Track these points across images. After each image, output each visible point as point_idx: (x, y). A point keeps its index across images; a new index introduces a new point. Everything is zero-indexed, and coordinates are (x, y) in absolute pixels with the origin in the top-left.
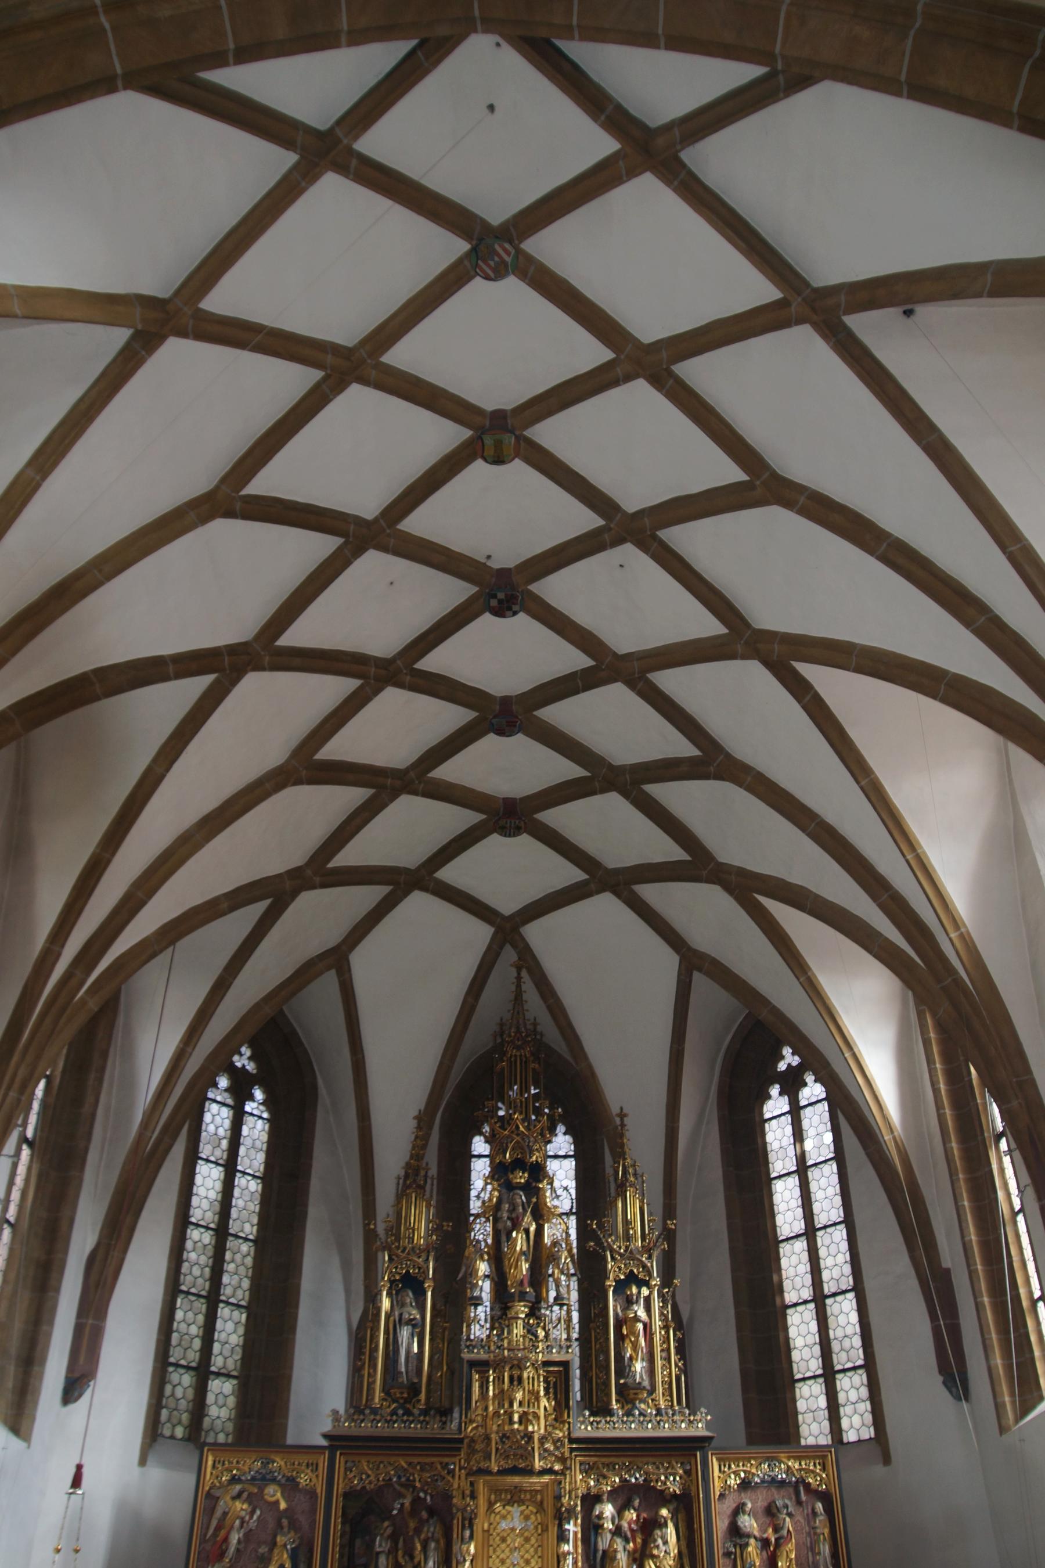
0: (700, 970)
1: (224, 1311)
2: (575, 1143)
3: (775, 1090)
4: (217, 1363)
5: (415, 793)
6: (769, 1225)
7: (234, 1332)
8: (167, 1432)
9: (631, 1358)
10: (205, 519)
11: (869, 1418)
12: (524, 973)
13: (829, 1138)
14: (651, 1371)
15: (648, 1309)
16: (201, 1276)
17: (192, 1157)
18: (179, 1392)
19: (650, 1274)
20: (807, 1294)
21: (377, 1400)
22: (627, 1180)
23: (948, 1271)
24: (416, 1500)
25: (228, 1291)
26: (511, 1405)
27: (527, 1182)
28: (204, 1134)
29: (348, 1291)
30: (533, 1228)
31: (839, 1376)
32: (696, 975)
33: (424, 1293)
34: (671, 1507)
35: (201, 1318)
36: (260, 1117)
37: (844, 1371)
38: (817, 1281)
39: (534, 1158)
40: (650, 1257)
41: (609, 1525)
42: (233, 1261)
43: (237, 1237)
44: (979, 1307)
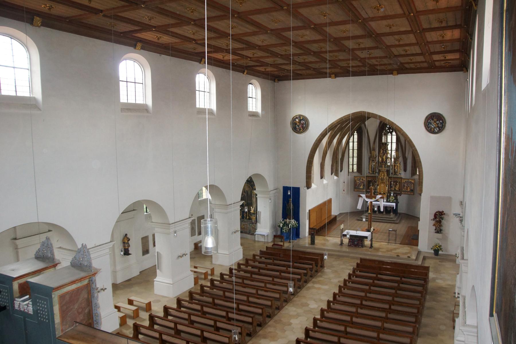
1: (354, 158)
4: (354, 164)
8: (350, 171)
24: (375, 181)
30: (386, 155)
35: (352, 160)
41: (392, 184)
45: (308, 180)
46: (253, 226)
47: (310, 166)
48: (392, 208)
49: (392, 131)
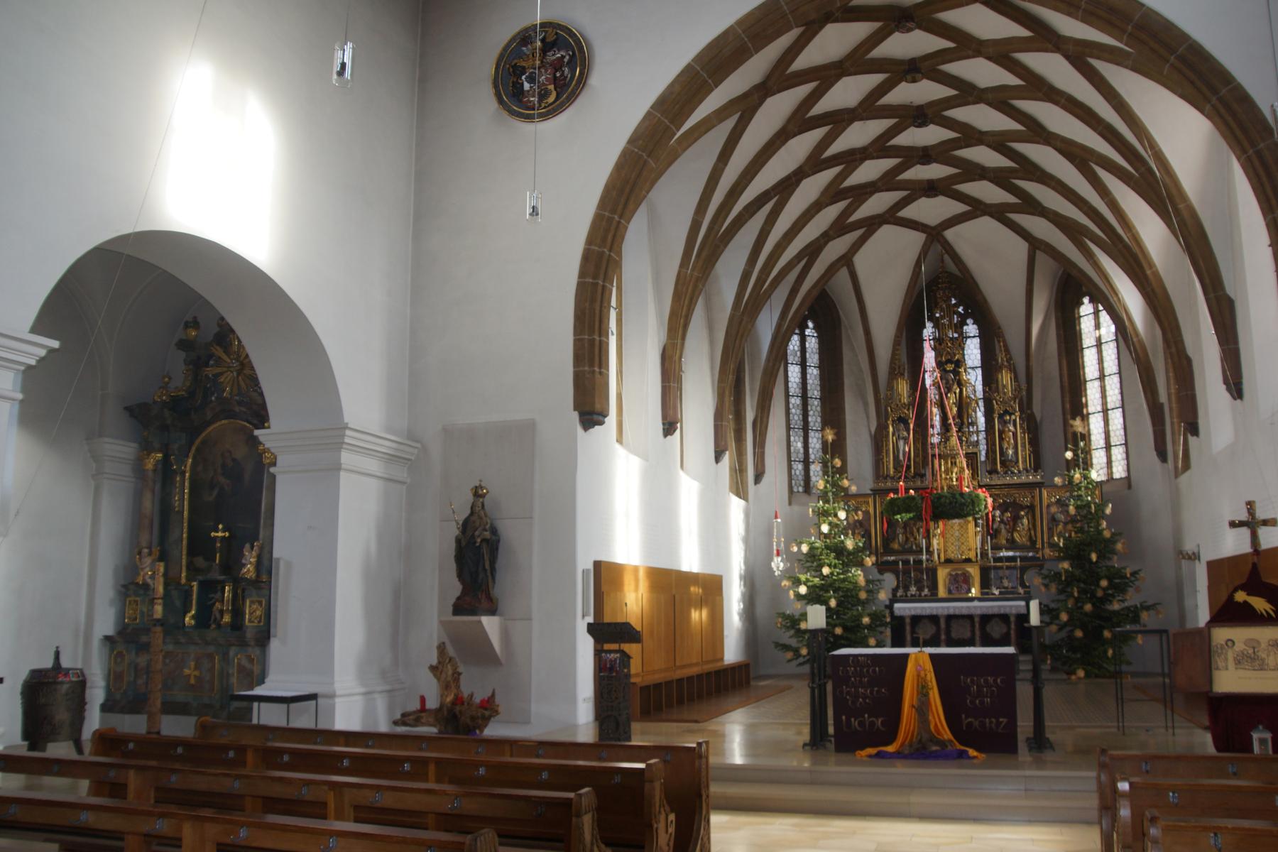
0: (1039, 249)
1: (811, 434)
2: (979, 329)
3: (1086, 300)
4: (812, 457)
5: (882, 191)
6: (1082, 373)
7: (818, 442)
8: (795, 490)
9: (1007, 448)
10: (784, 143)
11: (1125, 467)
12: (946, 257)
13: (1113, 328)
14: (1016, 453)
15: (1015, 426)
16: (799, 419)
17: (786, 364)
18: (798, 473)
19: (1015, 411)
20: (1099, 408)
21: (892, 473)
22: (1003, 364)
23: (1162, 404)
25: (811, 424)
26: (952, 474)
27: (954, 369)
28: (788, 351)
29: (868, 417)
30: (958, 391)
31: (1113, 448)
32: (1037, 251)
33: (909, 424)
34: (1026, 511)
35: (801, 438)
36: (813, 336)
37: (1116, 445)
38: (1104, 403)
39: (957, 357)
40: (1015, 402)
42: (812, 410)
43: (811, 398)
44: (1172, 423)
45: (587, 368)
46: (245, 662)
47: (597, 283)
48: (1012, 619)
49: (963, 323)
